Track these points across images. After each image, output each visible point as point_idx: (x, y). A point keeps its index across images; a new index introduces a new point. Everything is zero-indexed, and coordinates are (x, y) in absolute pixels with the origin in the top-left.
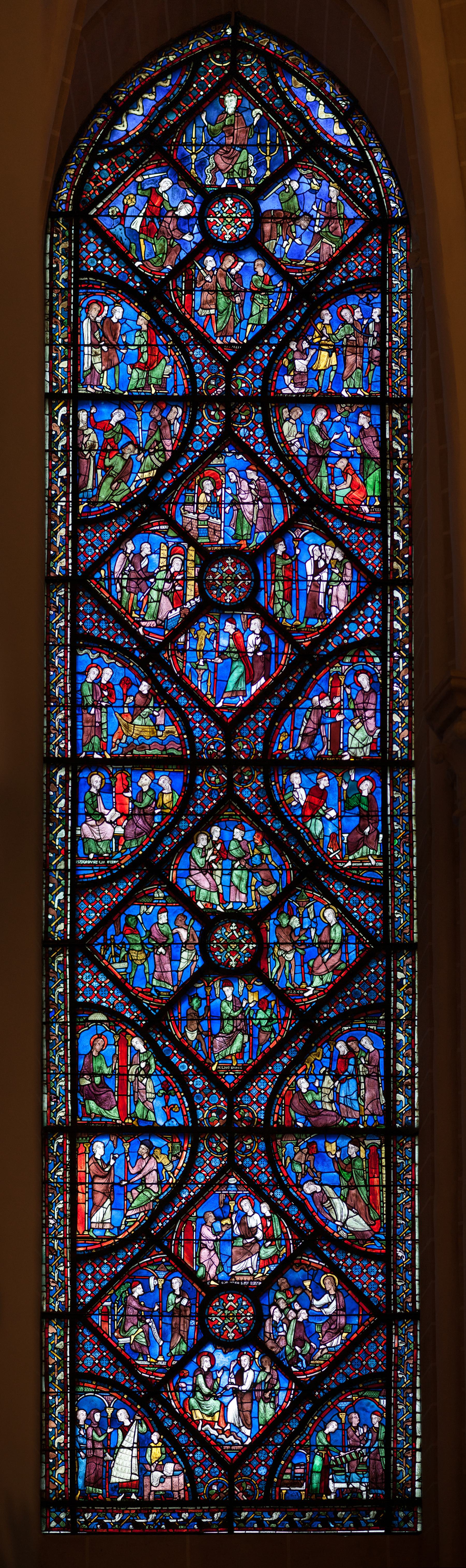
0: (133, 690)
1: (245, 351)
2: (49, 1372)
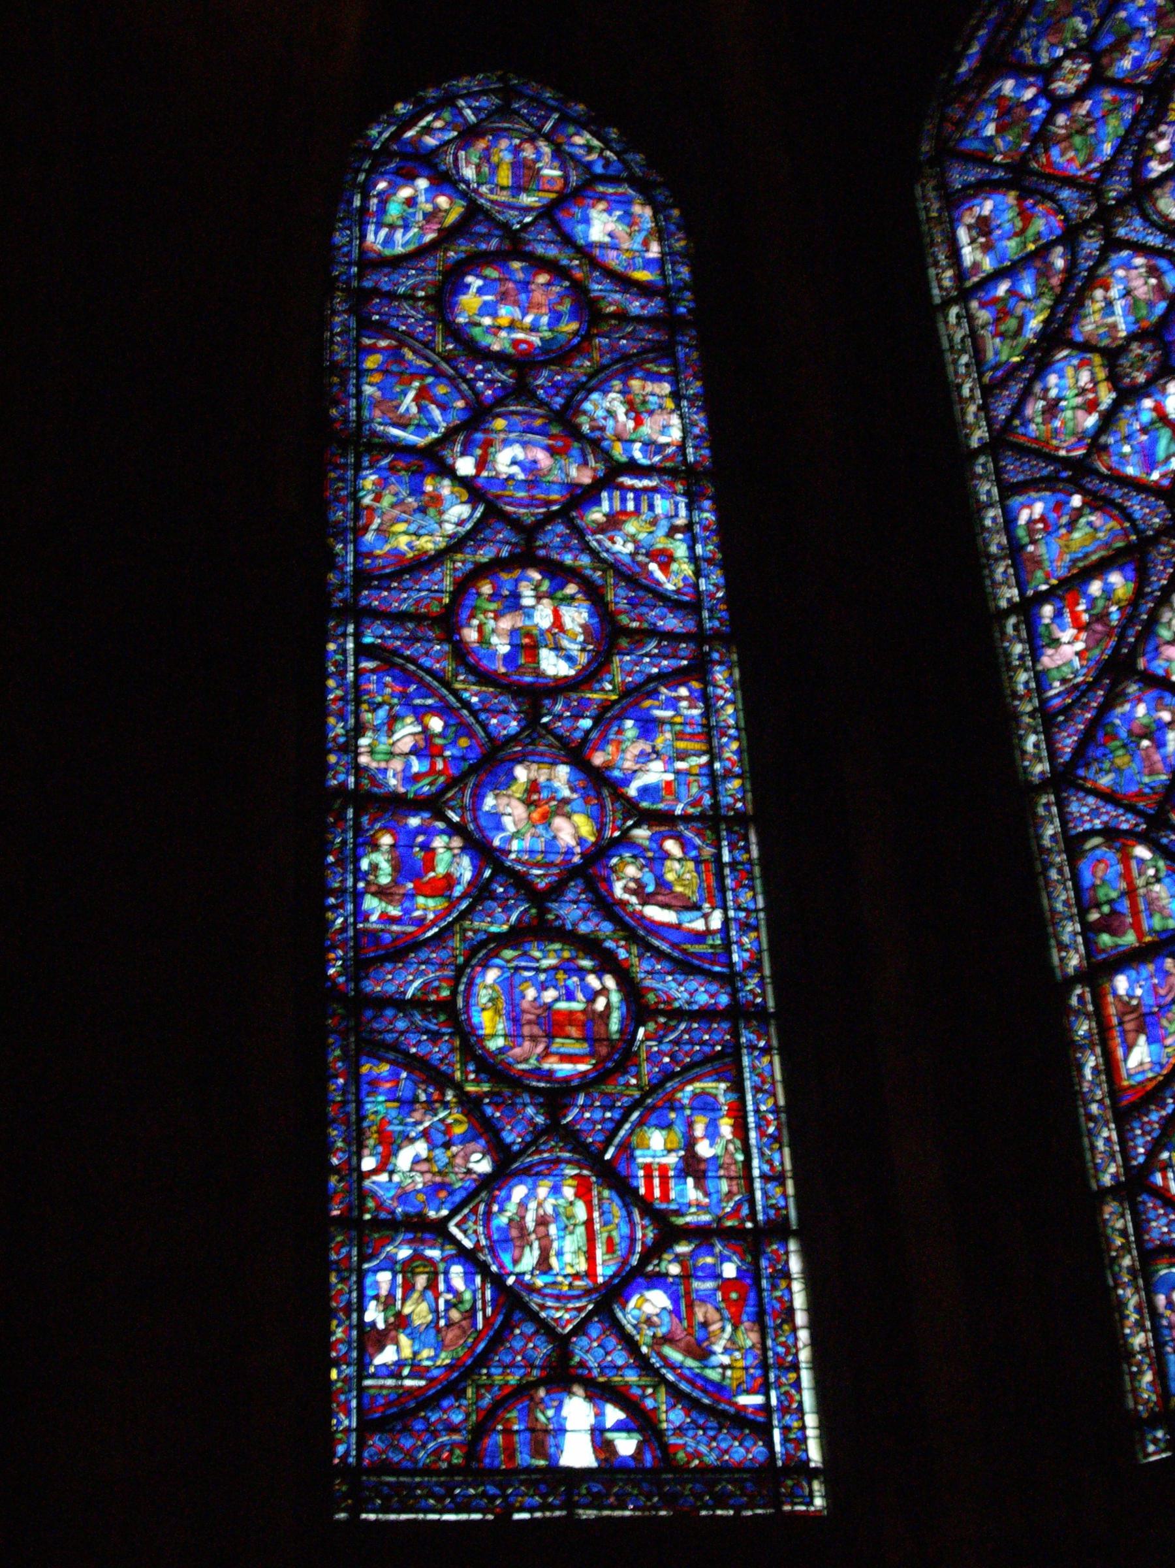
0: (1066, 509)
1: (1108, 169)
2: (1114, 1260)
